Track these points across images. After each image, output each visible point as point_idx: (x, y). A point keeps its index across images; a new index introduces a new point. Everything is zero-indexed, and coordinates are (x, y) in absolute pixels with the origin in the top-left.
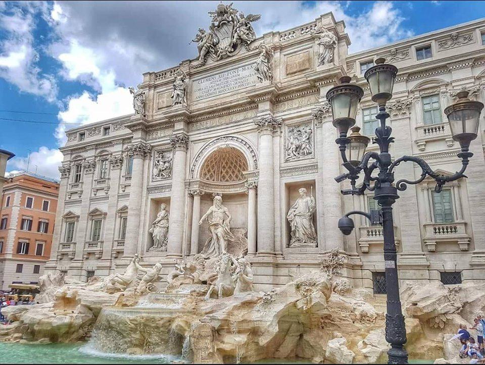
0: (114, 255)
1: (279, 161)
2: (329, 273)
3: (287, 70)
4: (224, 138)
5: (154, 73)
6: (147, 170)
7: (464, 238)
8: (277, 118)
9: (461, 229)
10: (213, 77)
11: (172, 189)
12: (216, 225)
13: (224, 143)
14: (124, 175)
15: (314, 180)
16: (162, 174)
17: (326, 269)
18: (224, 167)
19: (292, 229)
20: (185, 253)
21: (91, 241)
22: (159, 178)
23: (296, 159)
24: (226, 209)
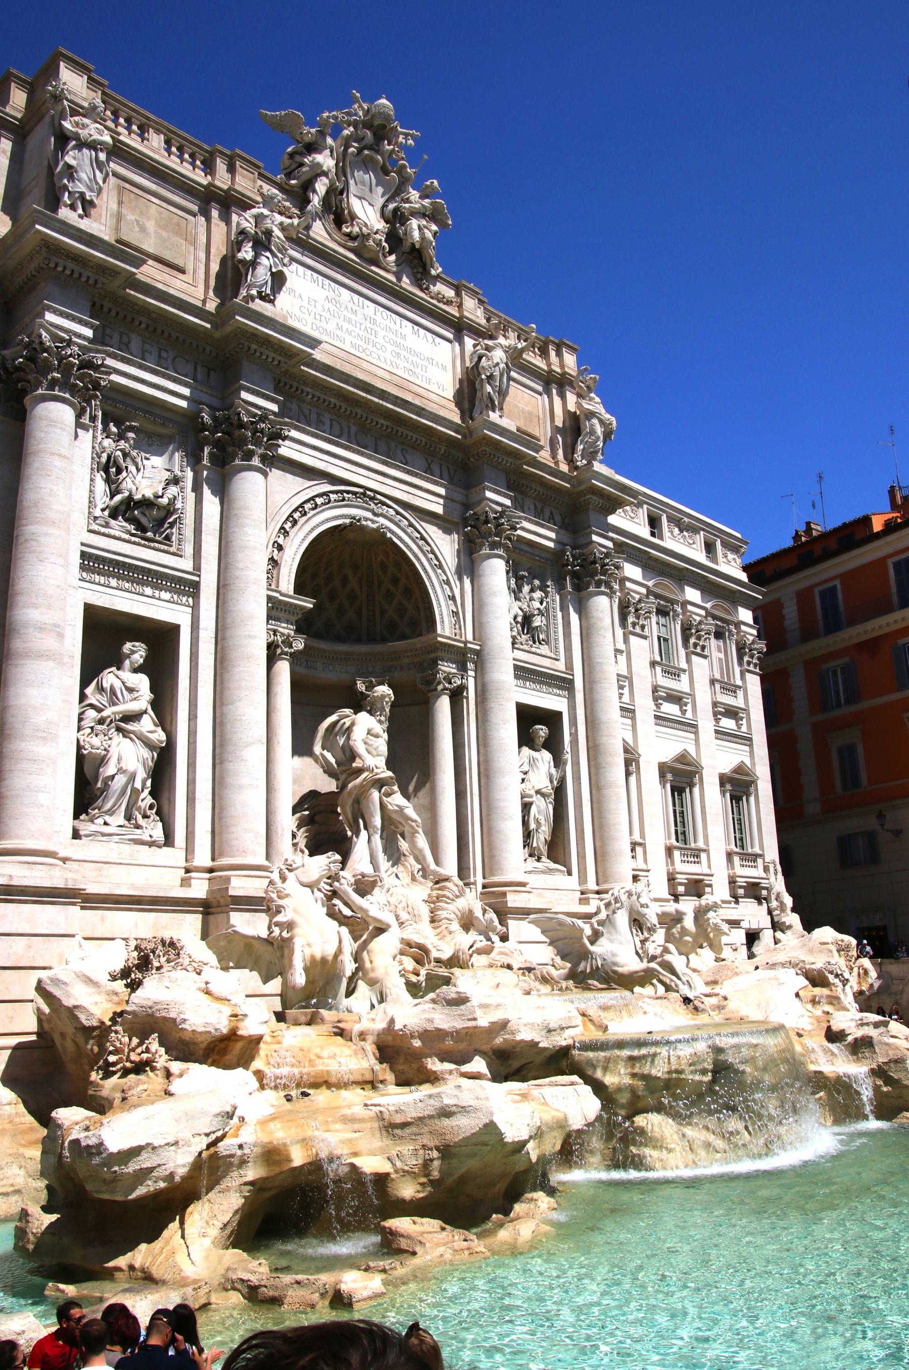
13: (369, 515)
15: (559, 714)
19: (533, 826)
23: (525, 647)
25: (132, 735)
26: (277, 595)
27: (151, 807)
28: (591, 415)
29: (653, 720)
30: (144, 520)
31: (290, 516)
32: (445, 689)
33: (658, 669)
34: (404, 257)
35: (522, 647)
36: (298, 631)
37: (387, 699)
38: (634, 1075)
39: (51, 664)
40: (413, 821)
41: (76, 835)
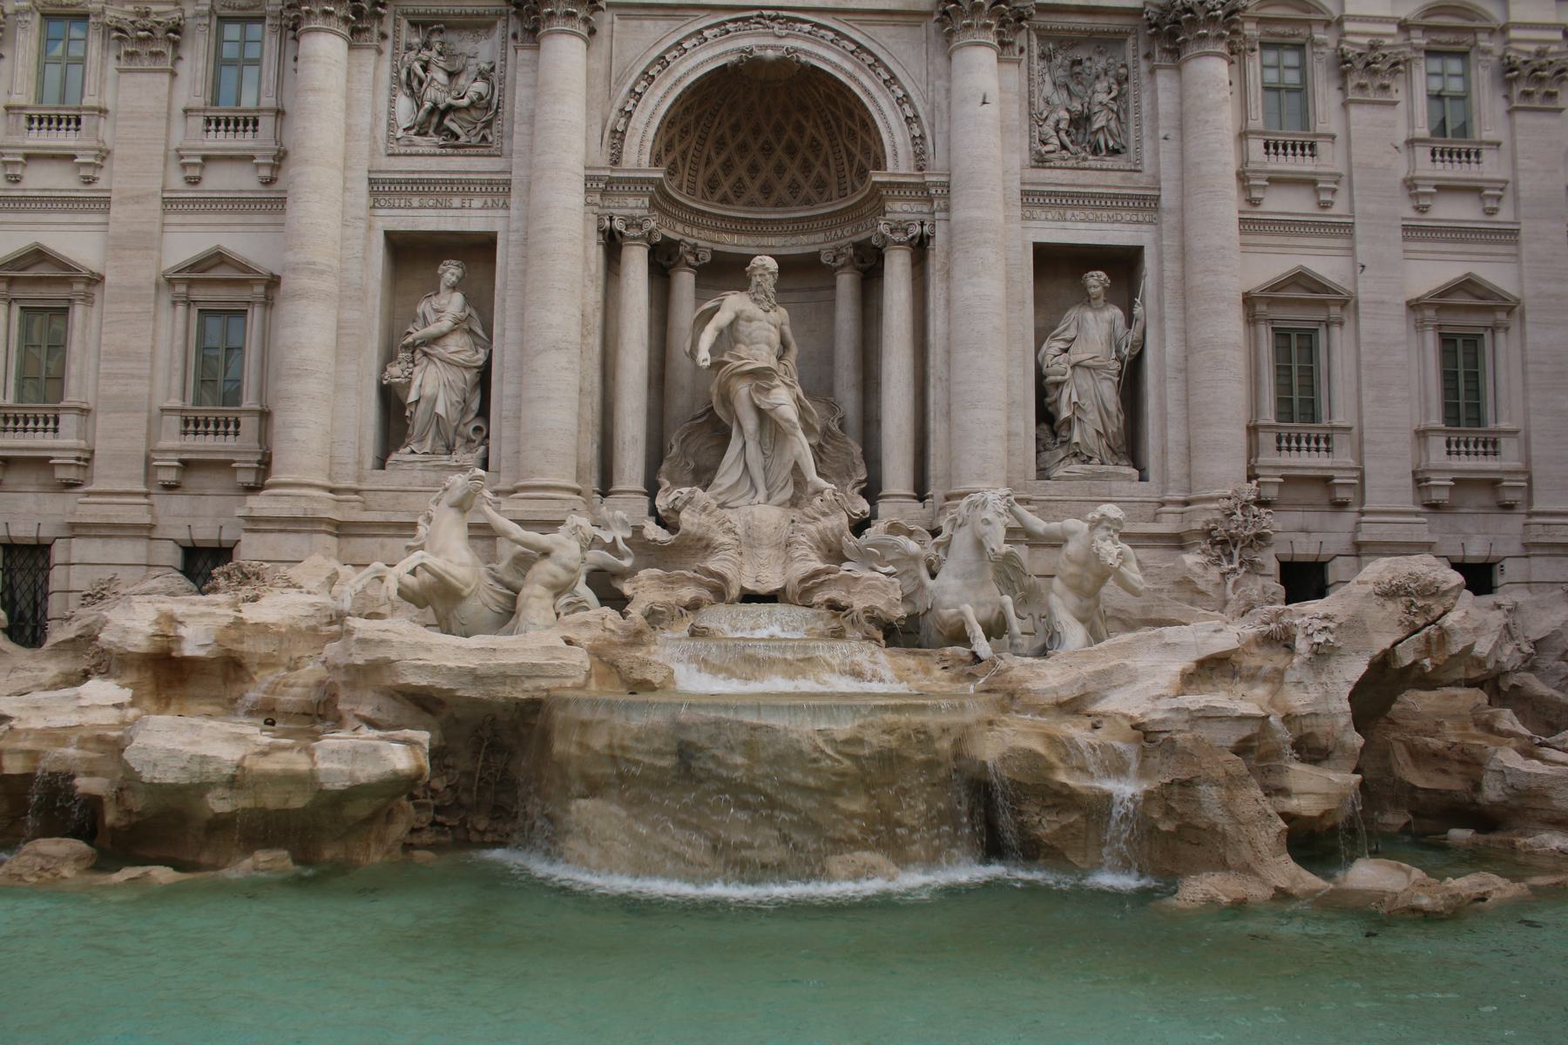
0: (170, 476)
1: (1019, 157)
2: (1230, 562)
4: (773, 19)
7: (1516, 472)
9: (1509, 447)
11: (514, 200)
12: (761, 376)
13: (772, 41)
14: (199, 102)
15: (1141, 248)
16: (440, 122)
17: (1218, 550)
18: (721, 144)
19: (1065, 413)
20: (593, 483)
21: (10, 401)
23: (1070, 163)
24: (783, 311)
27: (477, 429)
29: (1399, 233)
30: (454, 127)
31: (645, 72)
32: (899, 243)
33: (1423, 153)
35: (1058, 164)
37: (760, 271)
38: (581, 745)
39: (304, 302)
40: (788, 421)
41: (382, 463)
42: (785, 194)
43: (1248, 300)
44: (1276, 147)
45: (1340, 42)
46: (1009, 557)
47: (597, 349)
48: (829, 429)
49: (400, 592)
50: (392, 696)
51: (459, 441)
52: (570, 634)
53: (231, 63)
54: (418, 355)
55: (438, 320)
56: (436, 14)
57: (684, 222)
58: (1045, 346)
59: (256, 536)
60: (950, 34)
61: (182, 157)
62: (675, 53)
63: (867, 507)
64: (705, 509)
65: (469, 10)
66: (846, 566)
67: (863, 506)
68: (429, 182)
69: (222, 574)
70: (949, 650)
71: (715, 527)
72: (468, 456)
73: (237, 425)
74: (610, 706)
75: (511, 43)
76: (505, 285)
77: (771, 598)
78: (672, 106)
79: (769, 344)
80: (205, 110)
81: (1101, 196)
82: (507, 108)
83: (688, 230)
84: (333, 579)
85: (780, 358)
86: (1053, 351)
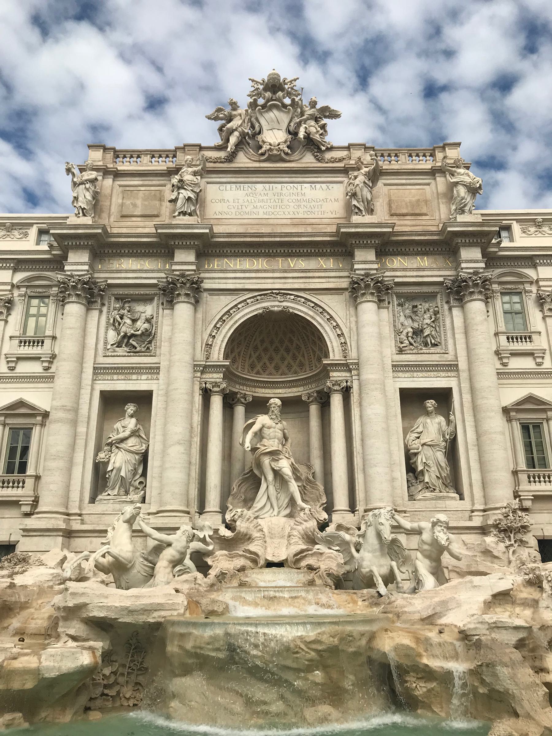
3: (390, 207)
4: (277, 295)
5: (114, 149)
6: (96, 330)
8: (386, 279)
10: (249, 185)
11: (161, 376)
13: (277, 303)
15: (450, 389)
16: (128, 342)
17: (502, 535)
18: (256, 348)
19: (420, 468)
22: (121, 351)
25: (122, 450)
26: (204, 363)
27: (141, 483)
28: (457, 183)
30: (134, 343)
31: (221, 318)
32: (337, 391)
34: (304, 149)
35: (409, 352)
36: (224, 379)
37: (273, 406)
38: (180, 647)
40: (288, 475)
41: (93, 500)
42: (287, 371)
43: (506, 411)
44: (512, 339)
45: (538, 290)
46: (394, 541)
47: (198, 443)
48: (308, 478)
49: (96, 566)
50: (86, 623)
51: (132, 489)
52: (178, 587)
53: (34, 316)
54: (114, 448)
55: (124, 431)
56: (127, 295)
57: (240, 384)
58: (408, 436)
59: (28, 538)
60: (356, 297)
61: (7, 358)
62: (234, 310)
63: (326, 516)
64: (248, 519)
65: (142, 293)
66: (317, 547)
67: (324, 516)
68: (122, 368)
69: (7, 560)
70: (365, 591)
71: (253, 528)
72: (136, 496)
73: (24, 483)
74: (195, 625)
75: (161, 307)
76: (156, 414)
77: (280, 565)
78: (233, 333)
79: (278, 439)
80: (19, 337)
81: (430, 366)
82: (159, 335)
83: (241, 387)
84: (64, 560)
85: (283, 445)
86: (412, 438)
